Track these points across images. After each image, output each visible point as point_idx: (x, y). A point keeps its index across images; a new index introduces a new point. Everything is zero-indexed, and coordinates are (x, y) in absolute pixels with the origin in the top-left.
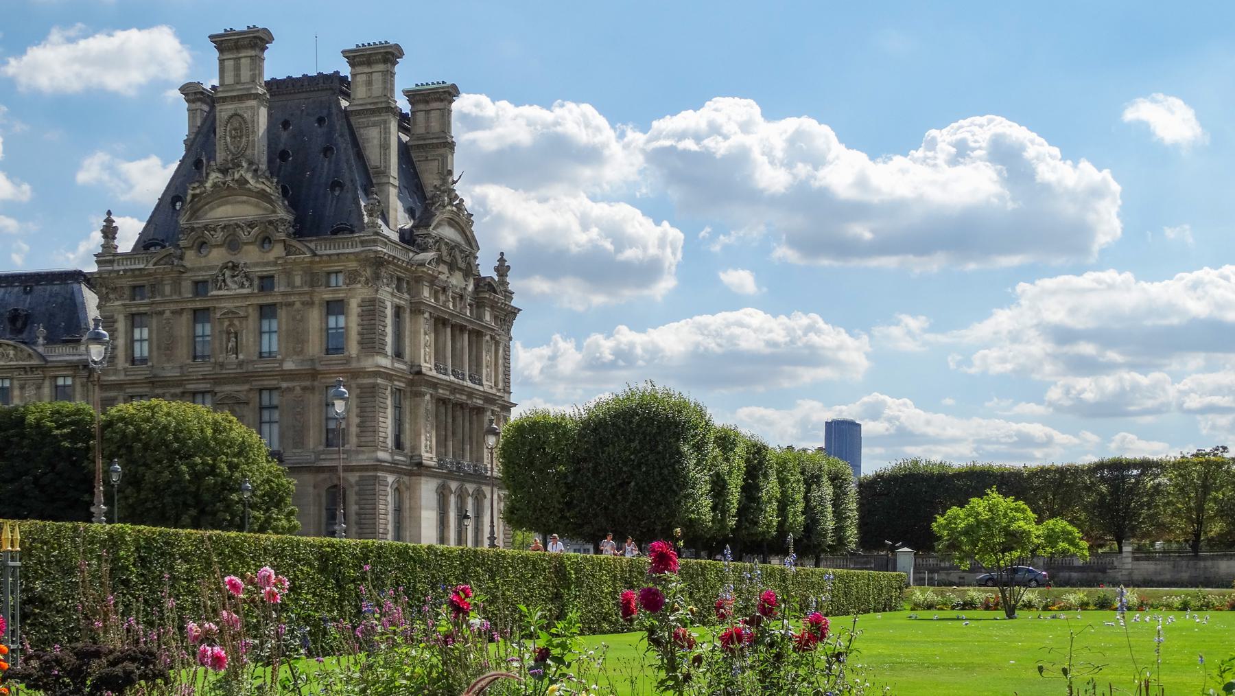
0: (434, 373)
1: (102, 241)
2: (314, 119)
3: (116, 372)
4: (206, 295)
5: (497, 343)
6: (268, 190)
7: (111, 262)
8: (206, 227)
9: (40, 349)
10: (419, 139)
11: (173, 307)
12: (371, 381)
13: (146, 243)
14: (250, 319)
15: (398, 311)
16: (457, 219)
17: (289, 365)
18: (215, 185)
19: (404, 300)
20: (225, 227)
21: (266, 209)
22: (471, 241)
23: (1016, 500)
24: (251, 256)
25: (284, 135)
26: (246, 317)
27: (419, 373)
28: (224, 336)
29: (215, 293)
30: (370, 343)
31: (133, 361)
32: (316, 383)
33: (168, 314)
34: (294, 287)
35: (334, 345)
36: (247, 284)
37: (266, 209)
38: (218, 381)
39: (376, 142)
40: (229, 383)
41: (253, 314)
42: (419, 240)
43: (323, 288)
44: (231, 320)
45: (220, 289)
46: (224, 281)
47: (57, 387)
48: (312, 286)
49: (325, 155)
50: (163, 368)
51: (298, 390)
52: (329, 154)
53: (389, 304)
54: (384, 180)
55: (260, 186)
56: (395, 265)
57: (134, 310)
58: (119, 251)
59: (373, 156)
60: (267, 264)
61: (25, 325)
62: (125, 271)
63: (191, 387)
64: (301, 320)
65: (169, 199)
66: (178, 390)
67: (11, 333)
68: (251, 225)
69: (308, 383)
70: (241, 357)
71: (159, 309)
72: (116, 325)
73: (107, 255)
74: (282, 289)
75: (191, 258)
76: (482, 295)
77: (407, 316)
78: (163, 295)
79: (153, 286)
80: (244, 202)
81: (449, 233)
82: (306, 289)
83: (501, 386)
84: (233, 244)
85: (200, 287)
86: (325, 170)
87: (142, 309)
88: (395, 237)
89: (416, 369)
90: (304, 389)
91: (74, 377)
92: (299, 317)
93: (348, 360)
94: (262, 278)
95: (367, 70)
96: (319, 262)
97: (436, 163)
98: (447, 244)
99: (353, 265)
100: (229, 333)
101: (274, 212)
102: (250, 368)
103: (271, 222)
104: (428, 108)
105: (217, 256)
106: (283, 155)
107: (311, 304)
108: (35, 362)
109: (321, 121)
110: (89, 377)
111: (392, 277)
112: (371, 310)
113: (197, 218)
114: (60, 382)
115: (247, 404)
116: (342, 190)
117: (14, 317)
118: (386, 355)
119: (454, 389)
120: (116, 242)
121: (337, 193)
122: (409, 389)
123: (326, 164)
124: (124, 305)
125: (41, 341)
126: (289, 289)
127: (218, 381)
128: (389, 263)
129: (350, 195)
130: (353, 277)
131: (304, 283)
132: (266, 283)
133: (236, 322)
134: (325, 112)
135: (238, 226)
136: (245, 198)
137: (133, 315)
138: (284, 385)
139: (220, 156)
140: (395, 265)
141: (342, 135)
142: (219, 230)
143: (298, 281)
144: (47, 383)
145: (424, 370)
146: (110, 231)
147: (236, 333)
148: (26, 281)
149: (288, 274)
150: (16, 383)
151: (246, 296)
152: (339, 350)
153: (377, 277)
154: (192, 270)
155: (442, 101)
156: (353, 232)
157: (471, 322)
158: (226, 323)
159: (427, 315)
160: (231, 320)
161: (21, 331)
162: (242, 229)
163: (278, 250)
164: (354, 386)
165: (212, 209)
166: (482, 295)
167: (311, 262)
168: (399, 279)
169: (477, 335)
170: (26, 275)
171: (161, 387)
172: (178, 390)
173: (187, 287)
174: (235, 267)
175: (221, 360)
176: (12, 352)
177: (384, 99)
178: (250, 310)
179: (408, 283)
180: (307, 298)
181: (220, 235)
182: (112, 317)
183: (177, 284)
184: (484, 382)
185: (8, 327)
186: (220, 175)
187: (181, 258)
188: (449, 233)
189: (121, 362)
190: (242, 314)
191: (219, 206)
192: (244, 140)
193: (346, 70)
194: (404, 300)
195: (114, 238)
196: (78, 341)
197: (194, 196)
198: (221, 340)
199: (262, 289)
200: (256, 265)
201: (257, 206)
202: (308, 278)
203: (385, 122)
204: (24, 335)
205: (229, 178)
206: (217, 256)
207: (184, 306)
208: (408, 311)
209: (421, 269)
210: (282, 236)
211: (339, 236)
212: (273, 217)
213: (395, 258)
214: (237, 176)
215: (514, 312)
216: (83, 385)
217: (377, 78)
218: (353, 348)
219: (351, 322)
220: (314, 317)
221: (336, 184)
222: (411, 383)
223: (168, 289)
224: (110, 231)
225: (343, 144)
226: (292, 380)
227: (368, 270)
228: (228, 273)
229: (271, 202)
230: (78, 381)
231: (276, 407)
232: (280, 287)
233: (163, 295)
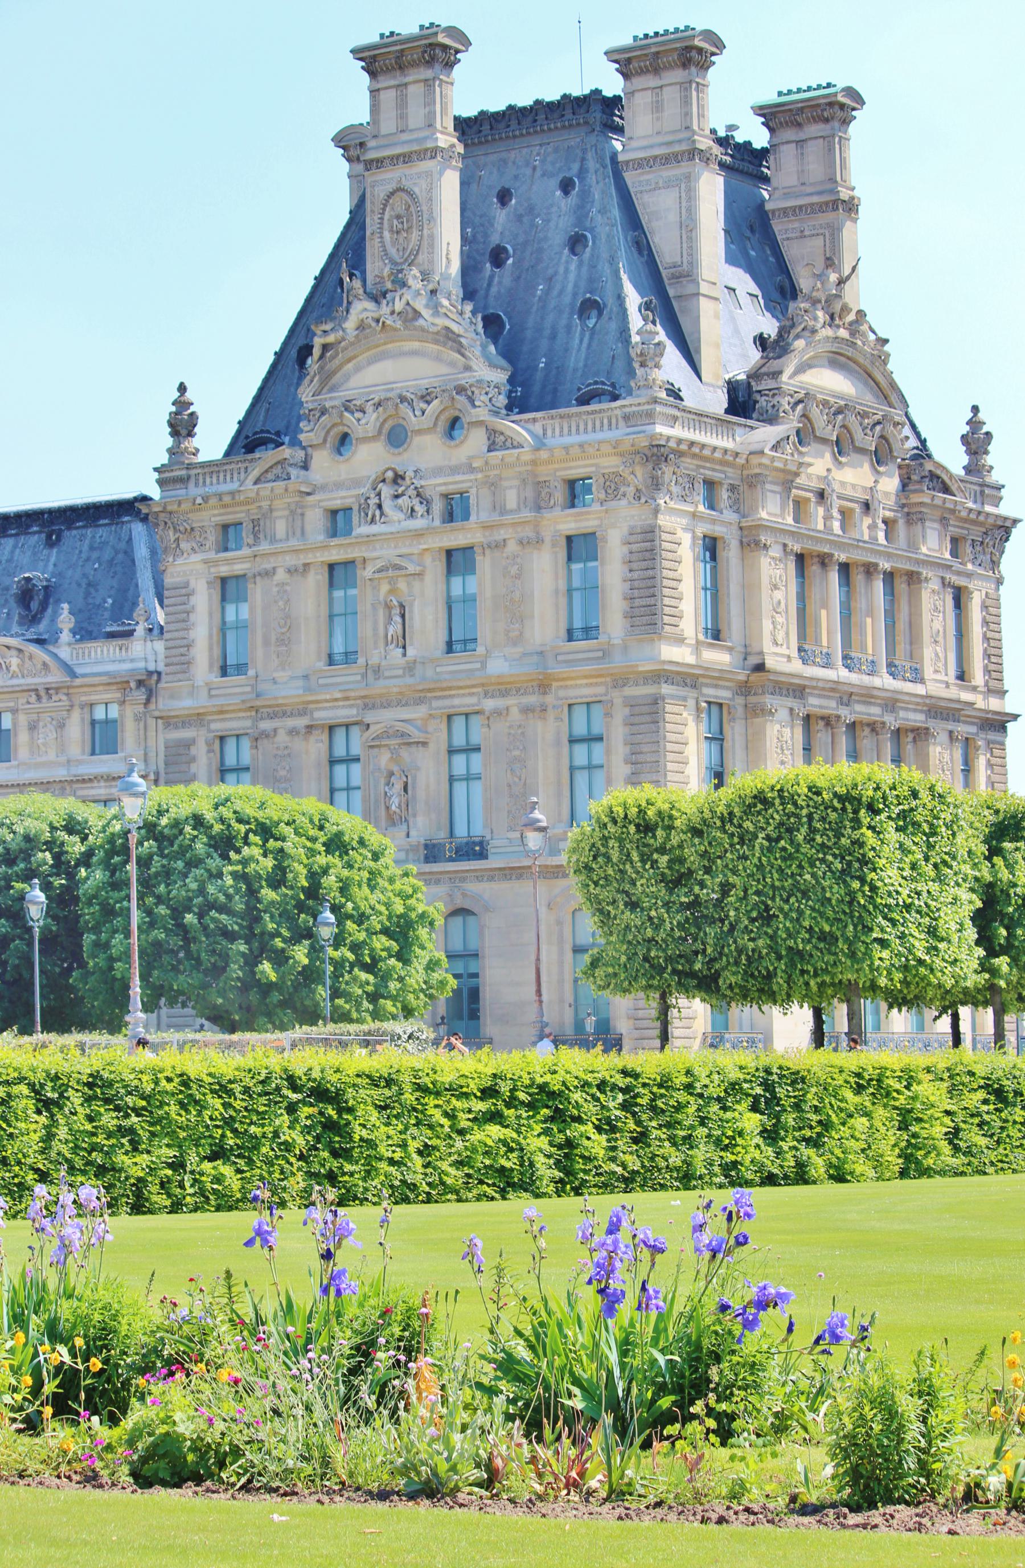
0: (796, 666)
1: (170, 442)
2: (554, 183)
3: (193, 690)
4: (348, 532)
5: (959, 598)
6: (455, 327)
7: (183, 481)
8: (347, 406)
9: (64, 652)
10: (786, 196)
11: (290, 560)
12: (649, 690)
13: (249, 440)
14: (428, 578)
15: (711, 547)
16: (850, 352)
17: (498, 667)
18: (361, 327)
19: (724, 524)
20: (379, 405)
21: (452, 364)
22: (888, 392)
23: (453, 991)
24: (428, 454)
25: (501, 217)
26: (420, 575)
27: (760, 668)
28: (381, 613)
29: (365, 529)
30: (647, 612)
31: (224, 671)
32: (549, 699)
33: (281, 575)
34: (503, 512)
36: (420, 509)
37: (452, 364)
39: (673, 217)
40: (387, 705)
41: (435, 568)
42: (762, 402)
43: (557, 512)
44: (392, 581)
45: (373, 521)
46: (380, 506)
47: (93, 723)
48: (538, 508)
49: (573, 251)
50: (274, 681)
51: (515, 713)
52: (579, 248)
53: (686, 538)
54: (690, 289)
55: (442, 322)
56: (694, 456)
57: (224, 570)
58: (201, 458)
60: (454, 470)
61: (44, 606)
62: (206, 499)
63: (324, 715)
64: (518, 577)
65: (294, 353)
66: (301, 722)
67: (20, 624)
68: (427, 397)
69: (532, 699)
70: (411, 652)
71: (268, 566)
72: (193, 600)
73: (177, 472)
74: (484, 516)
76: (915, 498)
77: (731, 554)
78: (273, 540)
79: (255, 523)
80: (414, 353)
81: (833, 383)
82: (527, 514)
83: (979, 678)
84: (397, 437)
85: (338, 520)
86: (572, 277)
87: (238, 568)
88: (718, 402)
89: (753, 660)
90: (526, 710)
91: (122, 703)
92: (514, 570)
93: (606, 653)
94: (447, 497)
95: (651, 81)
96: (549, 462)
97: (819, 242)
98: (825, 403)
99: (611, 463)
100: (388, 607)
101: (468, 368)
102: (429, 673)
103: (460, 390)
104: (802, 136)
105: (369, 459)
106: (498, 257)
108: (56, 677)
109: (566, 186)
110: (148, 701)
111: (692, 481)
112: (647, 550)
113: (332, 390)
114: (100, 714)
115: (424, 744)
116: (600, 314)
117: (26, 595)
119: (847, 696)
120: (195, 442)
121: (590, 324)
122: (740, 700)
123: (573, 267)
124: (205, 562)
125: (65, 636)
126: (496, 517)
127: (369, 704)
128: (681, 454)
129: (613, 326)
130: (613, 486)
131: (522, 503)
132: (455, 509)
133: (402, 585)
134: (575, 167)
135: (403, 399)
136: (416, 345)
137: (224, 580)
138: (489, 704)
140: (694, 456)
141: (603, 211)
142: (369, 408)
143: (511, 500)
144: (76, 715)
145: (770, 663)
146: (182, 424)
147: (402, 606)
148: (52, 523)
149: (493, 485)
150: (22, 718)
151: (419, 534)
152: (589, 632)
153: (656, 484)
154: (323, 488)
155: (827, 120)
156: (615, 398)
157: (889, 556)
158: (385, 588)
159: (776, 552)
160: (392, 581)
161: (34, 619)
162: (411, 403)
163: (475, 441)
164: (618, 702)
165: (358, 369)
166: (915, 498)
167: (534, 462)
168: (710, 485)
169: (901, 581)
170: (50, 512)
171: (272, 717)
172: (301, 722)
173: (315, 520)
174: (398, 478)
175: (374, 660)
176: (14, 662)
177: (684, 135)
178: (428, 559)
179: (733, 488)
180: (528, 532)
181: (372, 418)
182: (186, 585)
183: (296, 514)
184: (928, 673)
185: (17, 612)
186: (370, 305)
187: (305, 467)
188: (833, 383)
190: (412, 568)
191: (371, 362)
192: (415, 235)
193: (612, 85)
194: (724, 524)
195: (190, 434)
196: (130, 634)
197: (325, 347)
198: (375, 623)
199: (449, 517)
200: (438, 471)
201: (438, 358)
202: (529, 493)
203: (688, 177)
204: (43, 626)
205: (385, 310)
206: (369, 459)
207: (310, 558)
208: (734, 544)
209: (755, 460)
210: (481, 413)
211: (593, 407)
212: (465, 379)
213: (692, 444)
214: (399, 306)
216: (137, 719)
217: (671, 94)
218: (614, 623)
220: (545, 569)
221: (589, 307)
222: (744, 689)
223: (281, 528)
224: (182, 424)
225: (607, 225)
226: (504, 694)
227: (639, 471)
228: (386, 491)
229: (460, 349)
230: (129, 711)
231: (247, 769)
232: (480, 512)
233: (273, 540)
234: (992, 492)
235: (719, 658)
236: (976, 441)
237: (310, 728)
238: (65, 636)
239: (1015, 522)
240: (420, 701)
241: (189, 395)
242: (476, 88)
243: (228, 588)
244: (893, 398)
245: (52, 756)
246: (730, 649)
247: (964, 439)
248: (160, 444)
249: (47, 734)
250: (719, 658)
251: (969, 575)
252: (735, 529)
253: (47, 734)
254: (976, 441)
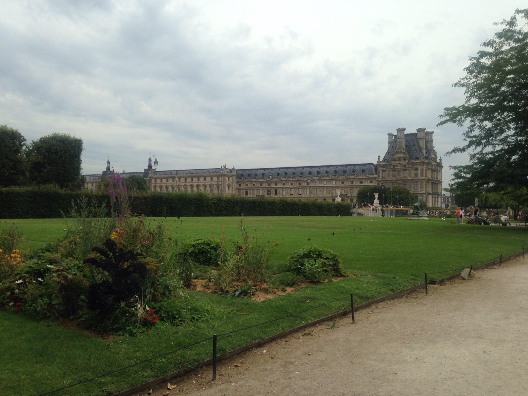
13: (384, 160)
17: (408, 178)
24: (402, 162)
35: (416, 175)
59: (421, 145)
75: (392, 162)
85: (394, 166)
139: (397, 147)
146: (379, 158)
189: (381, 177)
193: (417, 132)
206: (397, 162)
218: (419, 176)
219: (419, 172)
224: (379, 158)
242: (406, 132)
243: (383, 171)
248: (377, 160)
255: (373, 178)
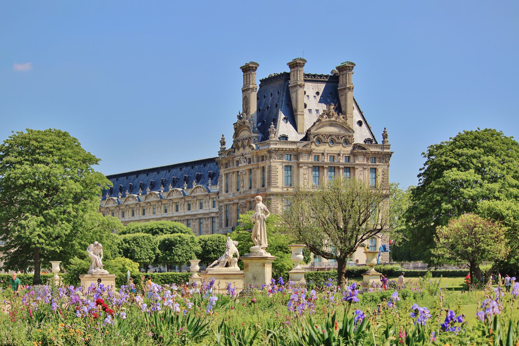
11: (232, 171)
15: (288, 168)
26: (246, 174)
38: (240, 199)
97: (344, 97)
103: (250, 138)
107: (258, 168)
109: (278, 93)
115: (246, 207)
118: (277, 187)
120: (225, 146)
125: (210, 184)
146: (223, 143)
151: (245, 166)
172: (232, 202)
174: (243, 155)
187: (234, 152)
189: (224, 193)
199: (250, 162)
206: (241, 150)
215: (390, 155)
220: (259, 173)
234: (388, 147)
235: (291, 190)
236: (385, 136)
237: (234, 204)
238: (210, 184)
239: (392, 153)
240: (245, 199)
241: (224, 137)
244: (350, 131)
245: (207, 208)
246: (293, 188)
247: (383, 135)
249: (207, 204)
250: (291, 190)
251: (378, 165)
252: (296, 164)
253: (207, 204)
254: (385, 136)
255: (214, 193)
